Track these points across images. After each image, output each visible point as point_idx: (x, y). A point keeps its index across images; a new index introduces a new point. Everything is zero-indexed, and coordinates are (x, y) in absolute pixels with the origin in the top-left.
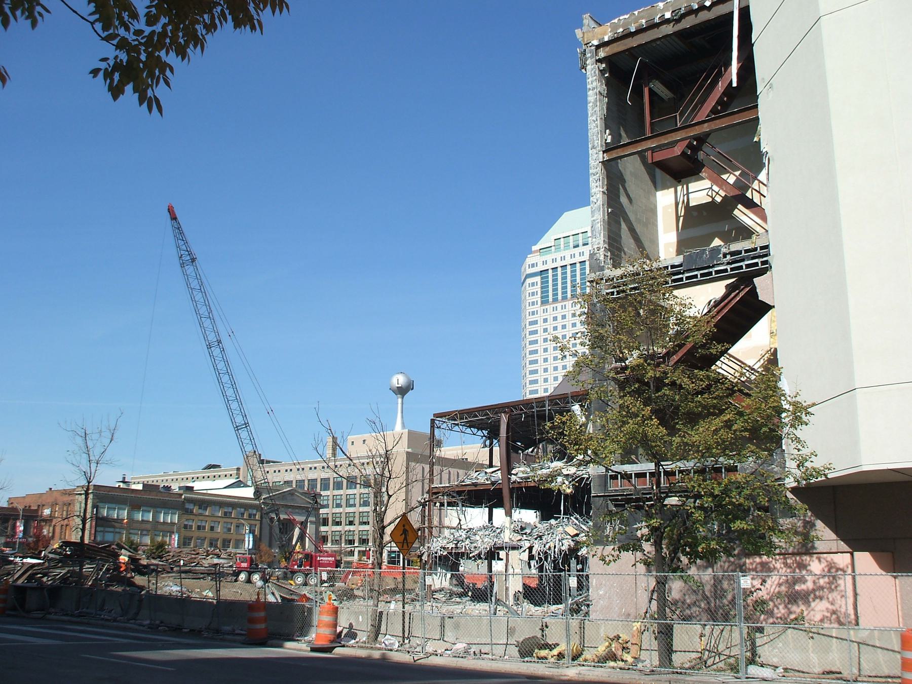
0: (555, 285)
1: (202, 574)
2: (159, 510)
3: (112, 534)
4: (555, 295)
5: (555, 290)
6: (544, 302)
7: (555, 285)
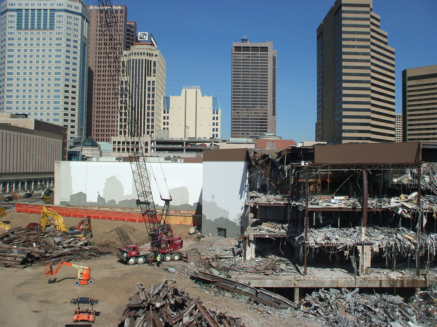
0: (27, 19)
1: (69, 255)
4: (26, 25)
5: (27, 22)
6: (19, 28)
7: (27, 19)
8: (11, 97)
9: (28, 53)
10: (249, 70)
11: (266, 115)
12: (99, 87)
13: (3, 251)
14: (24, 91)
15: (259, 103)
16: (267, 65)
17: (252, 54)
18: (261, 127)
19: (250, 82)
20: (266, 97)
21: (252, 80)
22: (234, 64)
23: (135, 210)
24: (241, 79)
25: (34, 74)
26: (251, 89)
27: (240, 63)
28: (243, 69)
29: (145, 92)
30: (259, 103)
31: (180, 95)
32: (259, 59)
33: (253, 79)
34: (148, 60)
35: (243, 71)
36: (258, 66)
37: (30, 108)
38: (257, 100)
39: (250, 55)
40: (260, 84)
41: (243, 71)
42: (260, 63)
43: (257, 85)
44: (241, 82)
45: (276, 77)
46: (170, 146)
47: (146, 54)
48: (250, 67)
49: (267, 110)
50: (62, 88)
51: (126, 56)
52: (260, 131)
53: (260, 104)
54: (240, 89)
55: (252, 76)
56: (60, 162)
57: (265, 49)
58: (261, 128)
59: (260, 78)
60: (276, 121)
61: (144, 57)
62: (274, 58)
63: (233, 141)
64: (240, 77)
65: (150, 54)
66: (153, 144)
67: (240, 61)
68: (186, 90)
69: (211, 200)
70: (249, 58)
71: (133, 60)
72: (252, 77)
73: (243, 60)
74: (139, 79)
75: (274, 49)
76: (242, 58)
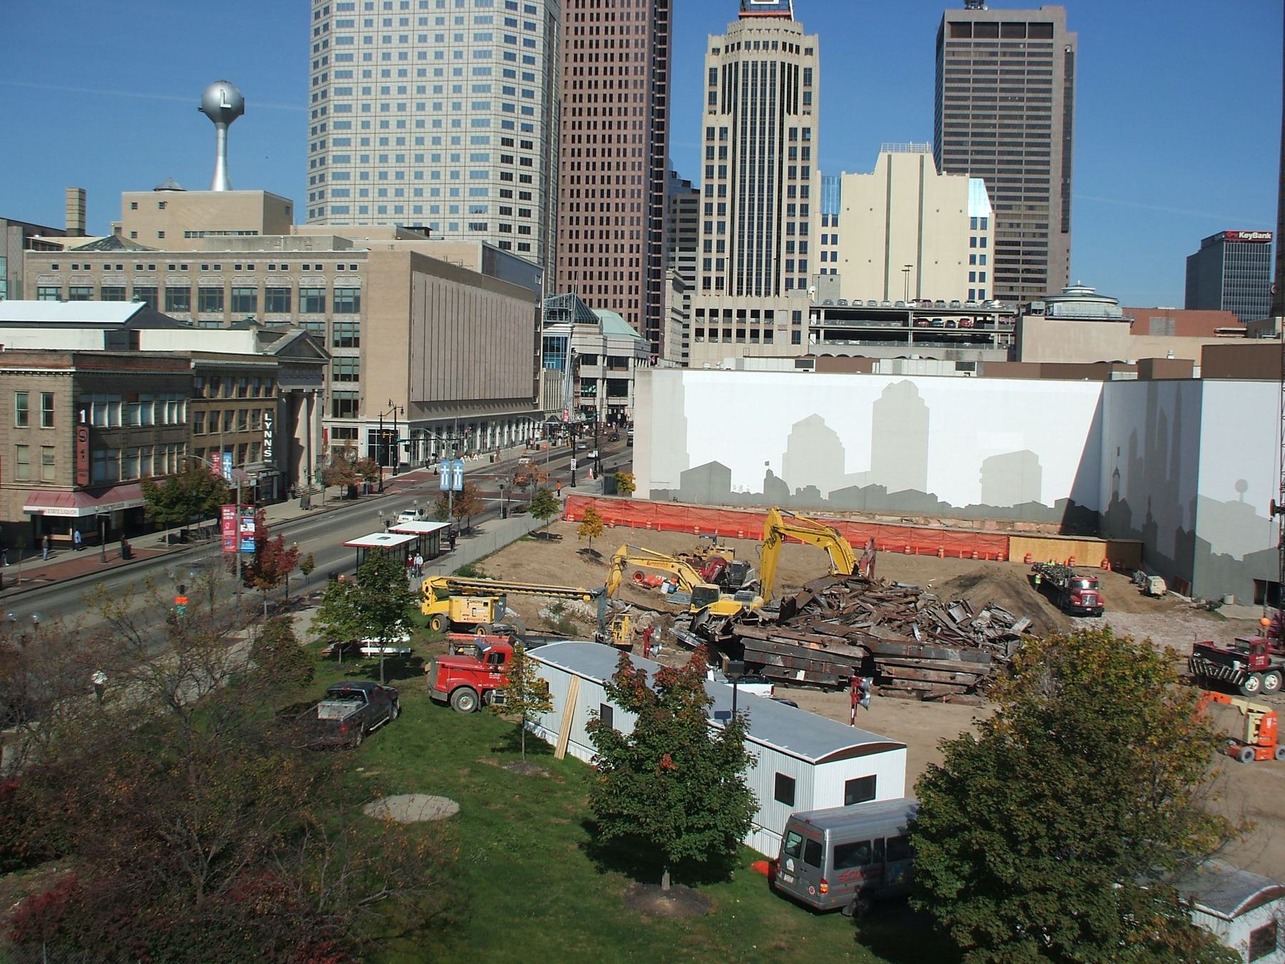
2: (162, 397)
3: (95, 464)
8: (346, 176)
9: (395, 48)
10: (993, 95)
11: (1044, 231)
12: (576, 146)
13: (916, 653)
14: (384, 159)
15: (1023, 194)
16: (1048, 77)
17: (1003, 45)
18: (1026, 266)
19: (997, 130)
20: (1045, 177)
21: (1001, 126)
22: (949, 76)
23: (878, 517)
24: (970, 121)
25: (411, 108)
26: (1001, 153)
27: (968, 72)
28: (975, 90)
29: (781, 163)
30: (1023, 194)
31: (870, 170)
32: (1026, 59)
33: (1006, 122)
34: (790, 66)
35: (975, 99)
36: (1022, 81)
37: (435, 210)
38: (1018, 185)
39: (999, 49)
40: (1029, 136)
41: (975, 99)
42: (1030, 72)
43: (1019, 140)
44: (970, 130)
45: (1074, 115)
46: (868, 326)
47: (780, 46)
48: (998, 85)
49: (1046, 217)
50: (494, 150)
51: (716, 51)
52: (1024, 280)
53: (1027, 199)
54: (965, 152)
55: (1003, 113)
56: (650, 373)
57: (1045, 29)
58: (1028, 271)
59: (1029, 117)
60: (1072, 249)
61: (779, 56)
62: (1069, 57)
63: (1065, 313)
64: (966, 117)
65: (791, 46)
66: (814, 317)
67: (967, 67)
68: (890, 157)
69: (1235, 496)
70: (994, 59)
71: (746, 64)
72: (1002, 117)
73: (976, 63)
74: (762, 123)
75: (1070, 28)
76: (972, 59)
